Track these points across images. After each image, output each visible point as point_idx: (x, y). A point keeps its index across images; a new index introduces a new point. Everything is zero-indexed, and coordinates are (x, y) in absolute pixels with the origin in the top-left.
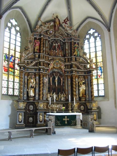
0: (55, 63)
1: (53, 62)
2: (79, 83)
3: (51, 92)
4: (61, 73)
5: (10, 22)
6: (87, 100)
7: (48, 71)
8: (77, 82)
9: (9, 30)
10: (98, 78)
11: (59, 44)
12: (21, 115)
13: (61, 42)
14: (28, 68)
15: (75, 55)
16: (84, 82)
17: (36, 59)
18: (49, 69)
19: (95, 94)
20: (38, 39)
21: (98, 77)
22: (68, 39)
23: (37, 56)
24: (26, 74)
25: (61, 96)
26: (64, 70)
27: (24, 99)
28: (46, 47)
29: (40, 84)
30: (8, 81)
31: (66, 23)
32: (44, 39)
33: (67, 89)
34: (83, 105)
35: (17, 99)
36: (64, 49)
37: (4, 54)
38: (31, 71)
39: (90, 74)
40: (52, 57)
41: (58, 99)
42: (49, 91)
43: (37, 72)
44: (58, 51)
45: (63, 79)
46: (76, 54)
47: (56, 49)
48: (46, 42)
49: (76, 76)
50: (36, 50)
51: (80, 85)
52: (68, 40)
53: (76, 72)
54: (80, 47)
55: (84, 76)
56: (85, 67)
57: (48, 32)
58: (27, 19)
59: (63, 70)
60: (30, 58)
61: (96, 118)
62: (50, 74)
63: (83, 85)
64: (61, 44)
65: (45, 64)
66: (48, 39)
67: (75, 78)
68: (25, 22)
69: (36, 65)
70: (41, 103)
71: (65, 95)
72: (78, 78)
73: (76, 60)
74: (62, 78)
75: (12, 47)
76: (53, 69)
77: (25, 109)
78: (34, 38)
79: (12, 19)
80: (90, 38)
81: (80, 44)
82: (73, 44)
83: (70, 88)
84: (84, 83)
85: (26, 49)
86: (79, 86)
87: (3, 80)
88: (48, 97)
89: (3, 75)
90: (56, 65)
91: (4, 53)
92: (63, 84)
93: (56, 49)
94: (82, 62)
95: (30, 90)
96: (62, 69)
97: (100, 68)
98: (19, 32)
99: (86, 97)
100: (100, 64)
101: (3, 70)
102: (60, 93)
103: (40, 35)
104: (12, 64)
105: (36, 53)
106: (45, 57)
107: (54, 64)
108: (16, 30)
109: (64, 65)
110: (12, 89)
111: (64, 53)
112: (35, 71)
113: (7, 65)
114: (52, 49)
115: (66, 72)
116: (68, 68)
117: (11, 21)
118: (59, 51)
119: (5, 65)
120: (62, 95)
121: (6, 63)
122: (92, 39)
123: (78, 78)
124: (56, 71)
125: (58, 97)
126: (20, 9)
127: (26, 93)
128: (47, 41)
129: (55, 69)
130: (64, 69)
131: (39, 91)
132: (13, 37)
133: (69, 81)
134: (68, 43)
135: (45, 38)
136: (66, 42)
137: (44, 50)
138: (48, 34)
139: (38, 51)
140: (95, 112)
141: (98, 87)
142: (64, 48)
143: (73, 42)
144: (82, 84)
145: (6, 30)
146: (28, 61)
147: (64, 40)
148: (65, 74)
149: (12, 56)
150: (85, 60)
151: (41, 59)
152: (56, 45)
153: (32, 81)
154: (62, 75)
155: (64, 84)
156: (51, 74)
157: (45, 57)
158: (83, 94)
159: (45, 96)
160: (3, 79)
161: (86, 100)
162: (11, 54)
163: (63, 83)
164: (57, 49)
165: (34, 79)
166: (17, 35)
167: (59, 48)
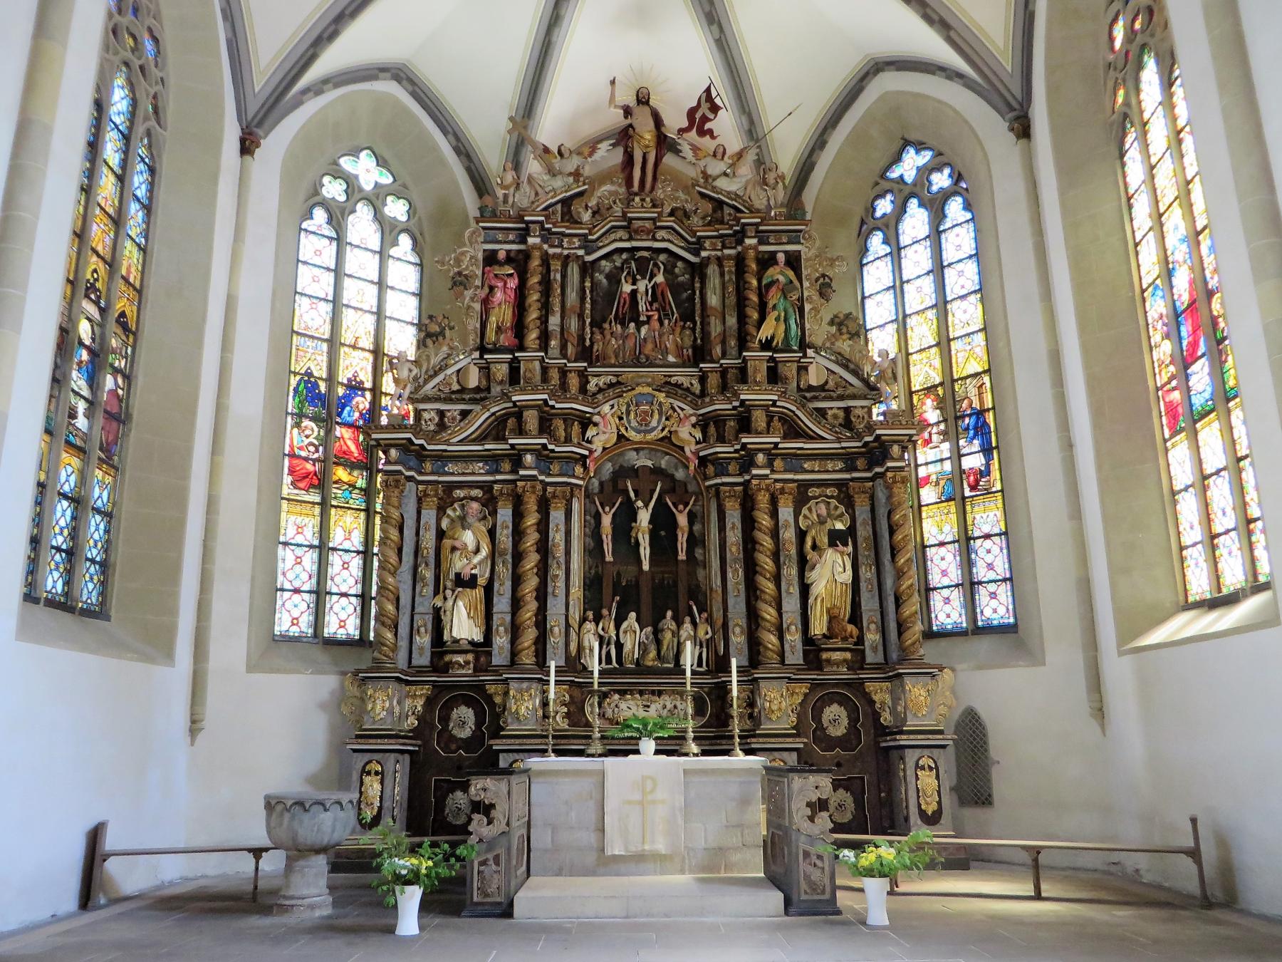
0: (628, 413)
1: (612, 406)
2: (801, 535)
3: (605, 612)
4: (680, 474)
5: (338, 174)
6: (870, 657)
7: (579, 470)
8: (789, 535)
9: (330, 222)
10: (964, 498)
11: (660, 278)
12: (377, 773)
13: (680, 264)
14: (443, 458)
15: (767, 345)
16: (839, 526)
17: (496, 390)
18: (591, 452)
19: (948, 611)
20: (510, 259)
21: (966, 486)
22: (722, 236)
23: (501, 371)
24: (426, 495)
25: (676, 634)
26: (696, 453)
27: (414, 662)
28: (568, 305)
29: (518, 557)
30: (323, 548)
31: (702, 133)
32: (555, 256)
33: (717, 582)
34: (843, 701)
35: (364, 660)
36: (698, 306)
37: (294, 381)
38: (464, 474)
39: (881, 465)
40: (607, 374)
41: (653, 654)
42: (594, 606)
43: (499, 477)
44: (656, 325)
45: (692, 517)
46: (773, 338)
47: (643, 318)
48: (564, 276)
49: (782, 491)
50: (491, 335)
51: (811, 555)
52: (724, 247)
53: (778, 463)
54: (806, 284)
55: (840, 484)
56: (848, 424)
57: (577, 207)
58: (457, 138)
59: (688, 453)
60: (456, 387)
61: (939, 803)
62: (601, 484)
63: (830, 551)
64: (681, 279)
65: (559, 424)
66: (581, 252)
67: (774, 502)
68: (442, 162)
69: (496, 430)
70: (525, 685)
71: (704, 631)
72: (801, 500)
73: (774, 376)
74: (681, 507)
75: (358, 327)
76: (622, 454)
77: (416, 733)
78: (480, 256)
79: (355, 152)
80: (901, 210)
81: (807, 260)
82: (754, 266)
83: (736, 576)
84: (836, 538)
85: (429, 335)
86: (803, 564)
87: (286, 544)
88: (586, 644)
89: (283, 515)
90: (634, 424)
91: (295, 374)
92: (690, 552)
93: (643, 318)
94: (822, 388)
95: (450, 603)
96: (682, 449)
97: (973, 419)
98: (406, 230)
99: (860, 640)
100: (973, 392)
101: (287, 479)
102: (669, 614)
103: (523, 235)
104: (356, 441)
105: (490, 352)
106: (555, 375)
107: (621, 418)
108: (379, 217)
109: (693, 419)
110: (353, 600)
111: (695, 339)
112: (488, 473)
113: (312, 449)
114: (612, 316)
115: (711, 469)
116: (721, 439)
117: (346, 163)
118: (661, 324)
119: (301, 448)
120: (687, 626)
121: (308, 432)
122: (916, 222)
123: (801, 500)
124: (643, 461)
125: (658, 643)
126: (399, 82)
127: (424, 621)
128: (574, 271)
129: (637, 450)
130: (693, 447)
131: (516, 604)
132: (361, 263)
133: (729, 526)
134: (721, 266)
135: (558, 250)
136: (708, 258)
137: (550, 328)
138: (576, 222)
139: (506, 339)
140: (926, 752)
141: (967, 563)
142: (694, 305)
143: (751, 253)
144: (826, 540)
145: (304, 225)
146: (441, 414)
147: (696, 248)
148: (707, 483)
149: (355, 387)
150: (846, 367)
151: (523, 391)
152: (642, 285)
153: (468, 538)
154: (686, 491)
155: (698, 552)
156: (608, 488)
157: (555, 375)
158: (832, 619)
159: (556, 639)
160: (282, 539)
161: (859, 661)
162: (343, 376)
163: (693, 541)
164: (649, 317)
165: (477, 524)
166: (394, 251)
167: (664, 313)
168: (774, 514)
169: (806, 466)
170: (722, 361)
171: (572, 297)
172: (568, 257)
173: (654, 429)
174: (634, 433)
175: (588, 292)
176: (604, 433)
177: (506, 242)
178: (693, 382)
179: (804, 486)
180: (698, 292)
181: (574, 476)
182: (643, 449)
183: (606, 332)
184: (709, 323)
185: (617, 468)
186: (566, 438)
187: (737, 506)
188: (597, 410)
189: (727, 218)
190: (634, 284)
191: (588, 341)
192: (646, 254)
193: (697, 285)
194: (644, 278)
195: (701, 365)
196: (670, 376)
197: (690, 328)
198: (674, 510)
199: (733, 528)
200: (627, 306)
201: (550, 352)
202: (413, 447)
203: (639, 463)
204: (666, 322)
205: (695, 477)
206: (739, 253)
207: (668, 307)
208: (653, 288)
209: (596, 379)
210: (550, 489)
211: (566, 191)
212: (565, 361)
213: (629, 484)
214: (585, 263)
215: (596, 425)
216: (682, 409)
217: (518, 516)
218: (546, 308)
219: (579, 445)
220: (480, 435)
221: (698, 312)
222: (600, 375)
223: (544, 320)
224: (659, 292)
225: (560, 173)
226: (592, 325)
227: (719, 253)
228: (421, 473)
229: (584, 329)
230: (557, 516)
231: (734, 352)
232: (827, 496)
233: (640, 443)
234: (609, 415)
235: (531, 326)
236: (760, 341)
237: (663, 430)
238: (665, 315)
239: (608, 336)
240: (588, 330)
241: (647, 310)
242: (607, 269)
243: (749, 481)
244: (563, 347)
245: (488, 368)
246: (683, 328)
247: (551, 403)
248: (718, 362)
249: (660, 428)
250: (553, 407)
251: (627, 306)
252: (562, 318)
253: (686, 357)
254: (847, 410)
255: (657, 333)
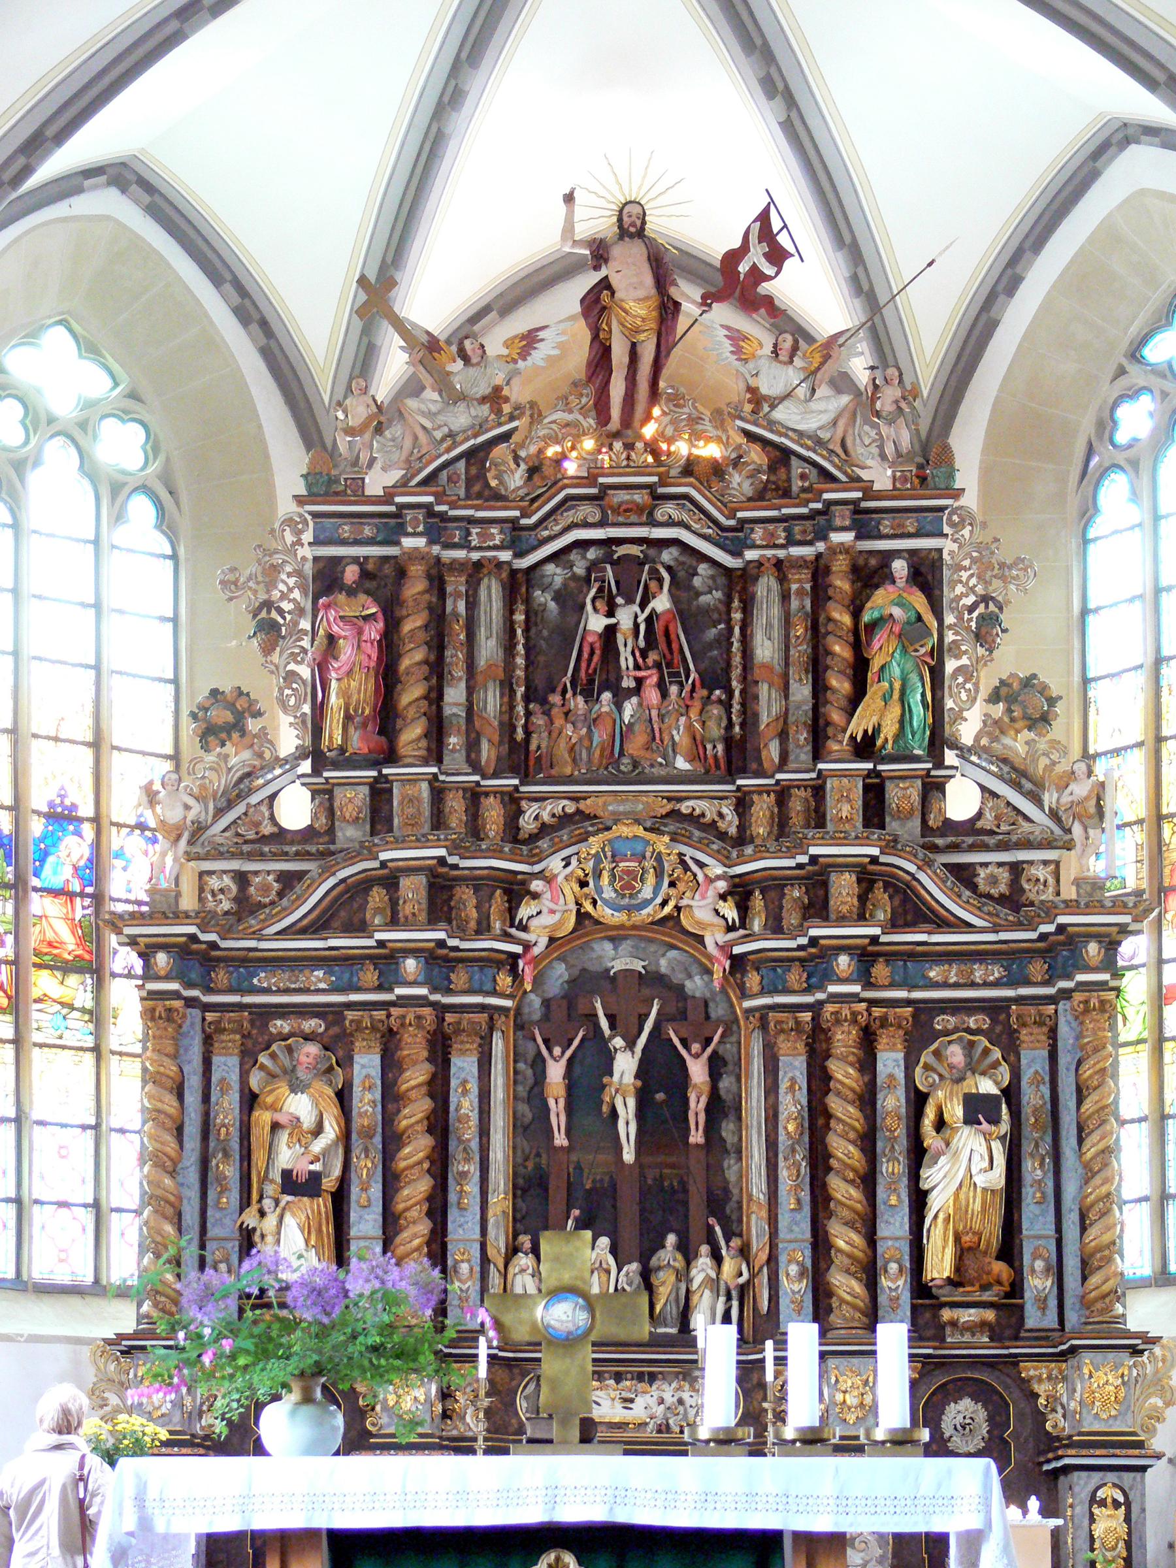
0: (598, 874)
2: (918, 1100)
4: (695, 985)
7: (504, 980)
8: (893, 1102)
11: (662, 603)
13: (703, 568)
14: (249, 962)
36: (737, 660)
45: (716, 1066)
47: (628, 683)
52: (791, 542)
66: (505, 556)
67: (868, 1040)
90: (608, 894)
96: (700, 939)
106: (456, 805)
109: (722, 886)
111: (730, 725)
112: (333, 990)
114: (567, 680)
116: (776, 927)
118: (664, 694)
128: (492, 594)
133: (784, 1085)
134: (782, 579)
135: (460, 554)
136: (759, 564)
137: (448, 711)
146: (242, 879)
148: (747, 1004)
150: (1016, 786)
156: (559, 1014)
157: (456, 805)
167: (669, 672)
168: (867, 1063)
169: (932, 974)
170: (779, 776)
171: (489, 648)
172: (478, 565)
173: (647, 902)
174: (609, 911)
175: (519, 632)
176: (552, 912)
177: (357, 542)
178: (725, 810)
179: (924, 1012)
180: (737, 630)
181: (494, 993)
182: (625, 938)
183: (555, 711)
184: (756, 697)
185: (576, 972)
186: (479, 923)
187: (801, 1046)
188: (537, 868)
189: (797, 484)
190: (610, 614)
191: (520, 731)
192: (635, 550)
193: (737, 616)
194: (630, 601)
195: (739, 782)
196: (680, 800)
197: (720, 701)
198: (683, 1052)
199: (791, 1089)
200: (596, 658)
201: (446, 759)
202: (195, 946)
203: (618, 965)
204: (674, 689)
205: (723, 990)
206: (819, 556)
207: (677, 658)
208: (649, 620)
209: (535, 805)
210: (450, 1018)
211: (475, 436)
212: (477, 778)
213: (598, 1005)
214: (514, 573)
215: (536, 896)
216: (701, 865)
217: (391, 1065)
218: (437, 670)
219: (506, 937)
220: (319, 918)
221: (736, 673)
222: (544, 799)
223: (435, 697)
224: (659, 627)
225: (461, 397)
226: (527, 699)
227: (781, 553)
228: (209, 990)
229: (512, 707)
230: (464, 1066)
231: (805, 755)
232: (969, 1031)
233: (622, 927)
234: (560, 879)
235: (411, 713)
236: (853, 738)
237: (664, 903)
238: (670, 675)
239: (559, 722)
240: (520, 709)
241: (637, 667)
242: (558, 581)
243: (821, 1003)
244: (472, 746)
245: (330, 792)
246: (707, 701)
247: (452, 860)
248: (772, 776)
249: (659, 900)
250: (455, 867)
251: (596, 658)
252: (470, 691)
253: (711, 761)
254: (1016, 869)
255: (654, 713)
